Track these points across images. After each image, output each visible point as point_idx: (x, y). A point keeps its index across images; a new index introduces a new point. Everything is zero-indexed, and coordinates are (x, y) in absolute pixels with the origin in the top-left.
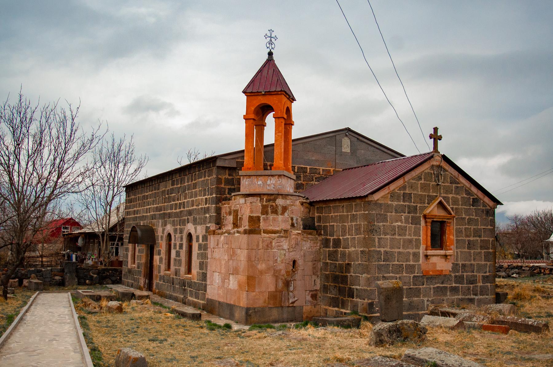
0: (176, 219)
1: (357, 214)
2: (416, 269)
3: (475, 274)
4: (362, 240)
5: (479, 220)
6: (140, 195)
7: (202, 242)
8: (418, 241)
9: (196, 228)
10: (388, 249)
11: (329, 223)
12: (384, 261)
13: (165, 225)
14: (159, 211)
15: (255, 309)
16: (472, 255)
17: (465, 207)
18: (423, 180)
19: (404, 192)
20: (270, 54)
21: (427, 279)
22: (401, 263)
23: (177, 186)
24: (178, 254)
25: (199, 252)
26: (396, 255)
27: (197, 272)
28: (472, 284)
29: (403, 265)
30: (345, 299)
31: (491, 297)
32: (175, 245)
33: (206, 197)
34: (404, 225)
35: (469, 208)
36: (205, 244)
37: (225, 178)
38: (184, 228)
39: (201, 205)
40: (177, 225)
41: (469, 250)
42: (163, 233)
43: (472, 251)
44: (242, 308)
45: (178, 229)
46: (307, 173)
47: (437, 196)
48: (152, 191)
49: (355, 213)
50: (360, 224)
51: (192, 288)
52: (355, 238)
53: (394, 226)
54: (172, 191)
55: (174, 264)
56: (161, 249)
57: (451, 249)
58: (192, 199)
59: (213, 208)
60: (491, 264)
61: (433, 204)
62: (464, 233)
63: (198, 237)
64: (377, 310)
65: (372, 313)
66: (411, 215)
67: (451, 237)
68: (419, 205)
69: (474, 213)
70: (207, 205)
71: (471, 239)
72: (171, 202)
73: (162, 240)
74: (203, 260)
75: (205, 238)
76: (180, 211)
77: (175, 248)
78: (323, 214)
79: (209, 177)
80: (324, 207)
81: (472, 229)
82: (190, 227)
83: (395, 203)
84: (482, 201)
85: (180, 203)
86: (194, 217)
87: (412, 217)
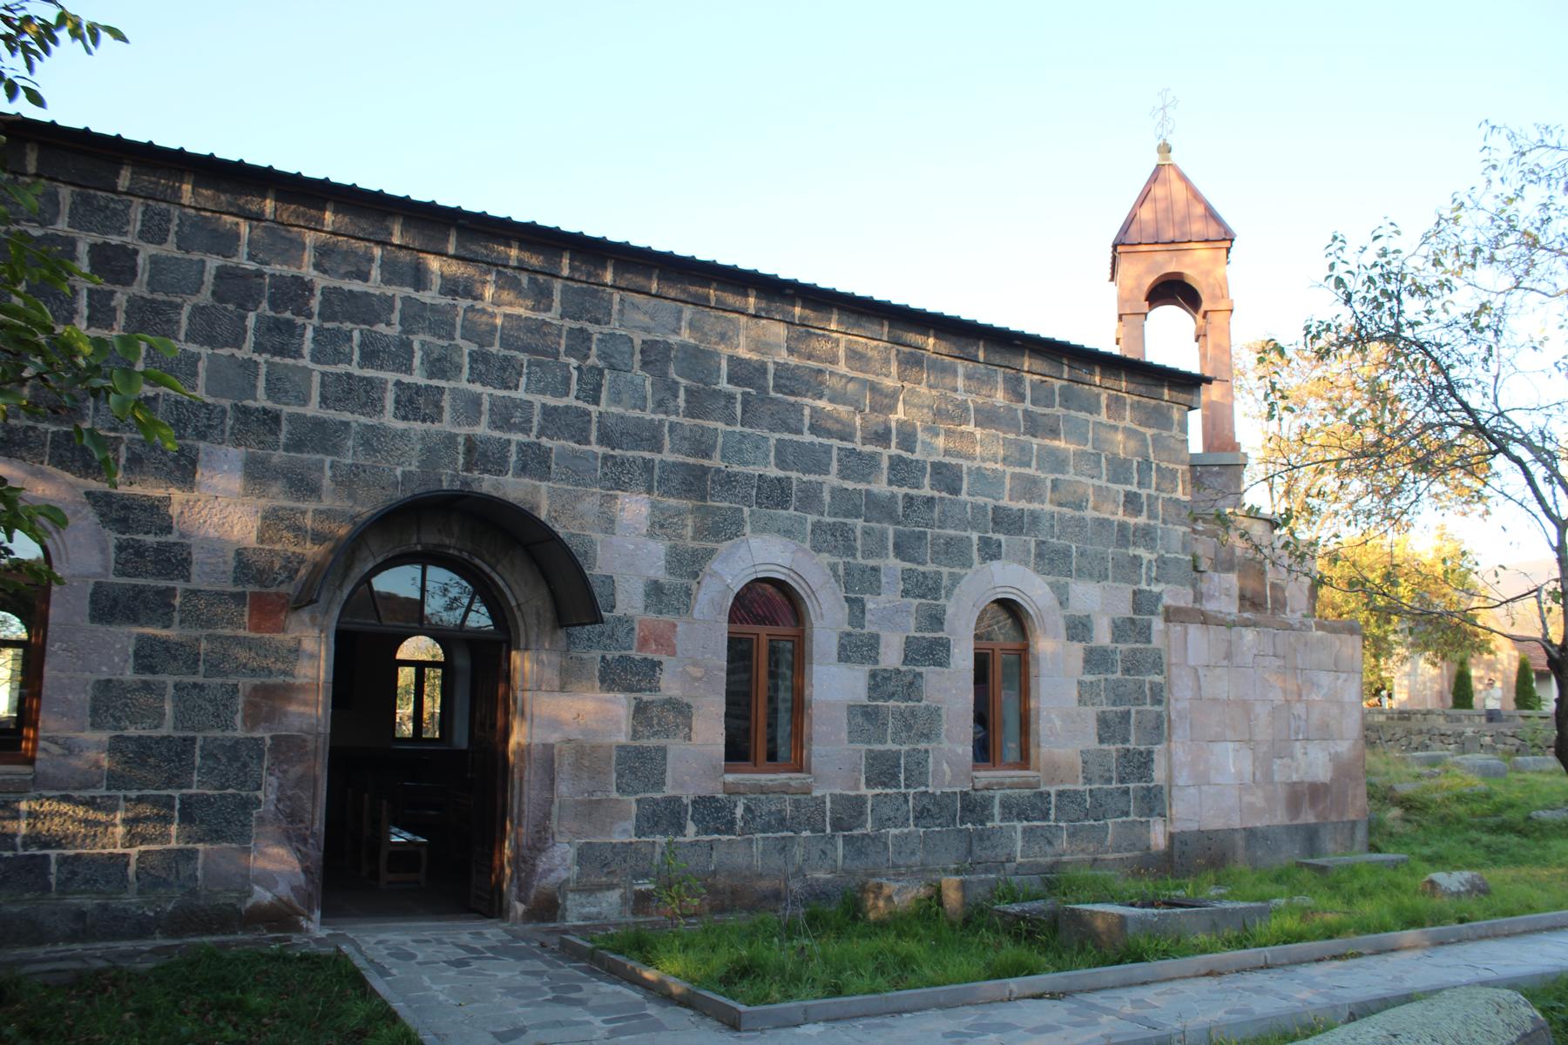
7: (1115, 640)
20: (1165, 149)
25: (1089, 678)
36: (1134, 651)
38: (955, 579)
56: (663, 658)
74: (1121, 708)
76: (909, 499)
86: (1040, 544)
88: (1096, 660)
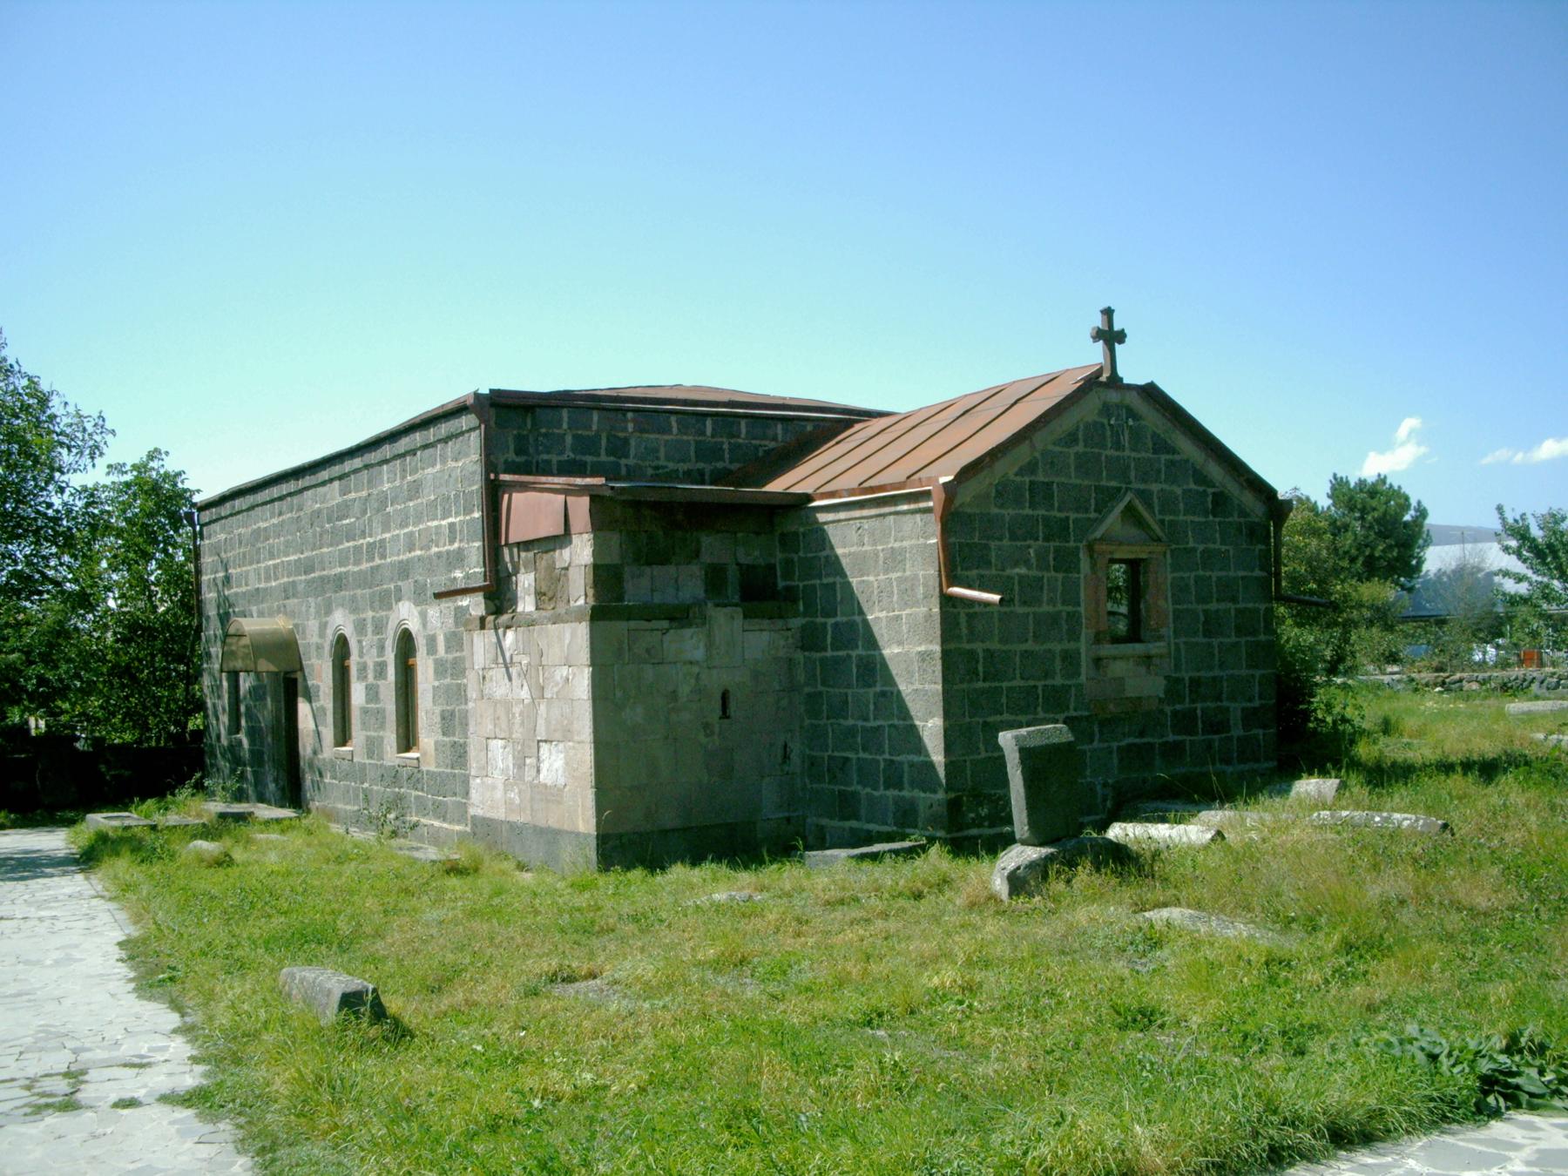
0: (359, 592)
1: (904, 550)
2: (1073, 699)
3: (1225, 704)
4: (922, 620)
5: (1231, 553)
6: (242, 530)
7: (446, 652)
8: (1073, 618)
9: (423, 616)
10: (995, 645)
11: (820, 579)
12: (984, 681)
13: (329, 612)
14: (305, 573)
15: (620, 836)
16: (1216, 652)
17: (1196, 519)
18: (1081, 443)
19: (1033, 478)
21: (1102, 724)
22: (1032, 683)
23: (359, 494)
24: (373, 694)
25: (437, 684)
26: (1018, 659)
27: (436, 743)
28: (1216, 732)
29: (1035, 687)
30: (876, 793)
31: (1266, 765)
32: (363, 668)
33: (451, 520)
34: (1034, 573)
35: (1202, 519)
37: (506, 462)
38: (388, 618)
39: (437, 546)
40: (364, 610)
41: (1206, 640)
42: (322, 635)
43: (1215, 642)
44: (586, 836)
45: (369, 621)
46: (739, 437)
47: (1119, 489)
48: (280, 514)
49: (897, 545)
50: (916, 576)
51: (422, 790)
52: (898, 618)
53: (1010, 578)
54: (343, 510)
55: (364, 723)
57: (1160, 638)
58: (406, 530)
59: (474, 551)
60: (1263, 675)
61: (1110, 511)
62: (1193, 589)
63: (432, 641)
64: (973, 819)
65: (960, 830)
66: (1052, 544)
67: (1161, 603)
68: (1073, 516)
69: (1218, 535)
70: (456, 545)
71: (1213, 606)
72: (342, 543)
73: (319, 656)
75: (454, 641)
77: (362, 676)
78: (801, 554)
79: (456, 460)
80: (804, 535)
81: (1214, 579)
82: (407, 614)
83: (1009, 512)
84: (1236, 502)
85: (369, 544)
87: (1057, 550)
88: (441, 669)
